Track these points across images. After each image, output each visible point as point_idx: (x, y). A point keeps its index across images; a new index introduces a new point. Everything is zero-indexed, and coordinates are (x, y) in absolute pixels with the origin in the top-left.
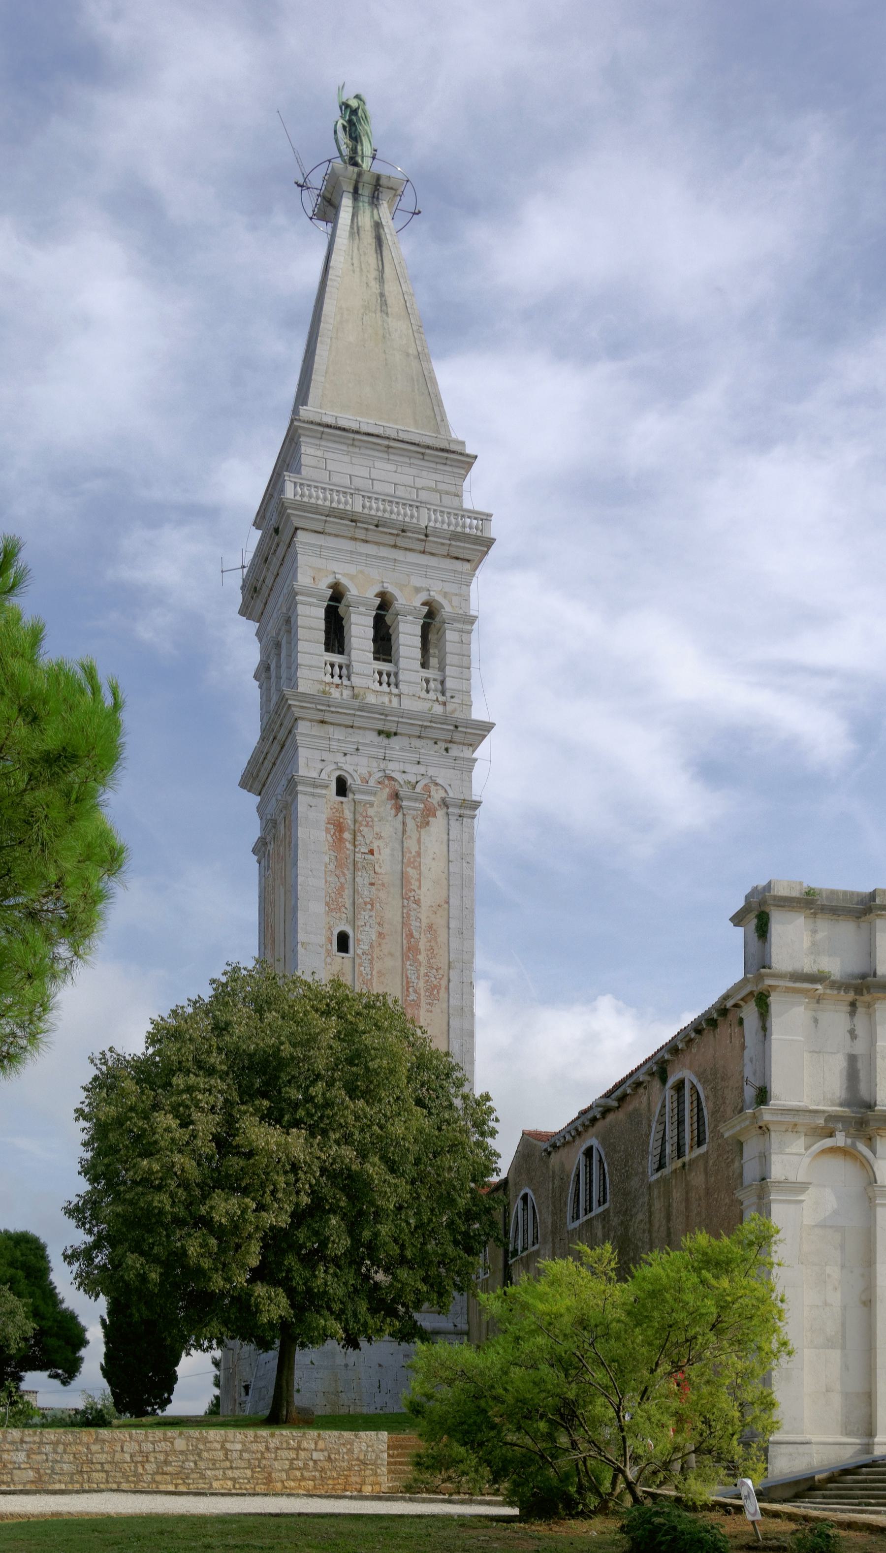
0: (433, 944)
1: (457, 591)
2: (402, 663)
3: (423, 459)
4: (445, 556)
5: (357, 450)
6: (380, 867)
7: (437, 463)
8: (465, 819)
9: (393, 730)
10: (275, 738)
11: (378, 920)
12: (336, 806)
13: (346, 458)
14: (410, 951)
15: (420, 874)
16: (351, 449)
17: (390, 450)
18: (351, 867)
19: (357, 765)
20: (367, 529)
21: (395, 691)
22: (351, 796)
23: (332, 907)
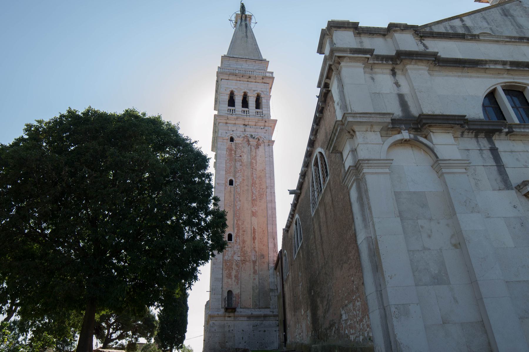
0: (261, 182)
1: (266, 90)
2: (250, 108)
6: (243, 160)
9: (247, 124)
10: (216, 132)
11: (243, 175)
14: (253, 184)
15: (256, 162)
17: (247, 62)
18: (234, 161)
19: (237, 133)
21: (248, 114)
22: (234, 141)
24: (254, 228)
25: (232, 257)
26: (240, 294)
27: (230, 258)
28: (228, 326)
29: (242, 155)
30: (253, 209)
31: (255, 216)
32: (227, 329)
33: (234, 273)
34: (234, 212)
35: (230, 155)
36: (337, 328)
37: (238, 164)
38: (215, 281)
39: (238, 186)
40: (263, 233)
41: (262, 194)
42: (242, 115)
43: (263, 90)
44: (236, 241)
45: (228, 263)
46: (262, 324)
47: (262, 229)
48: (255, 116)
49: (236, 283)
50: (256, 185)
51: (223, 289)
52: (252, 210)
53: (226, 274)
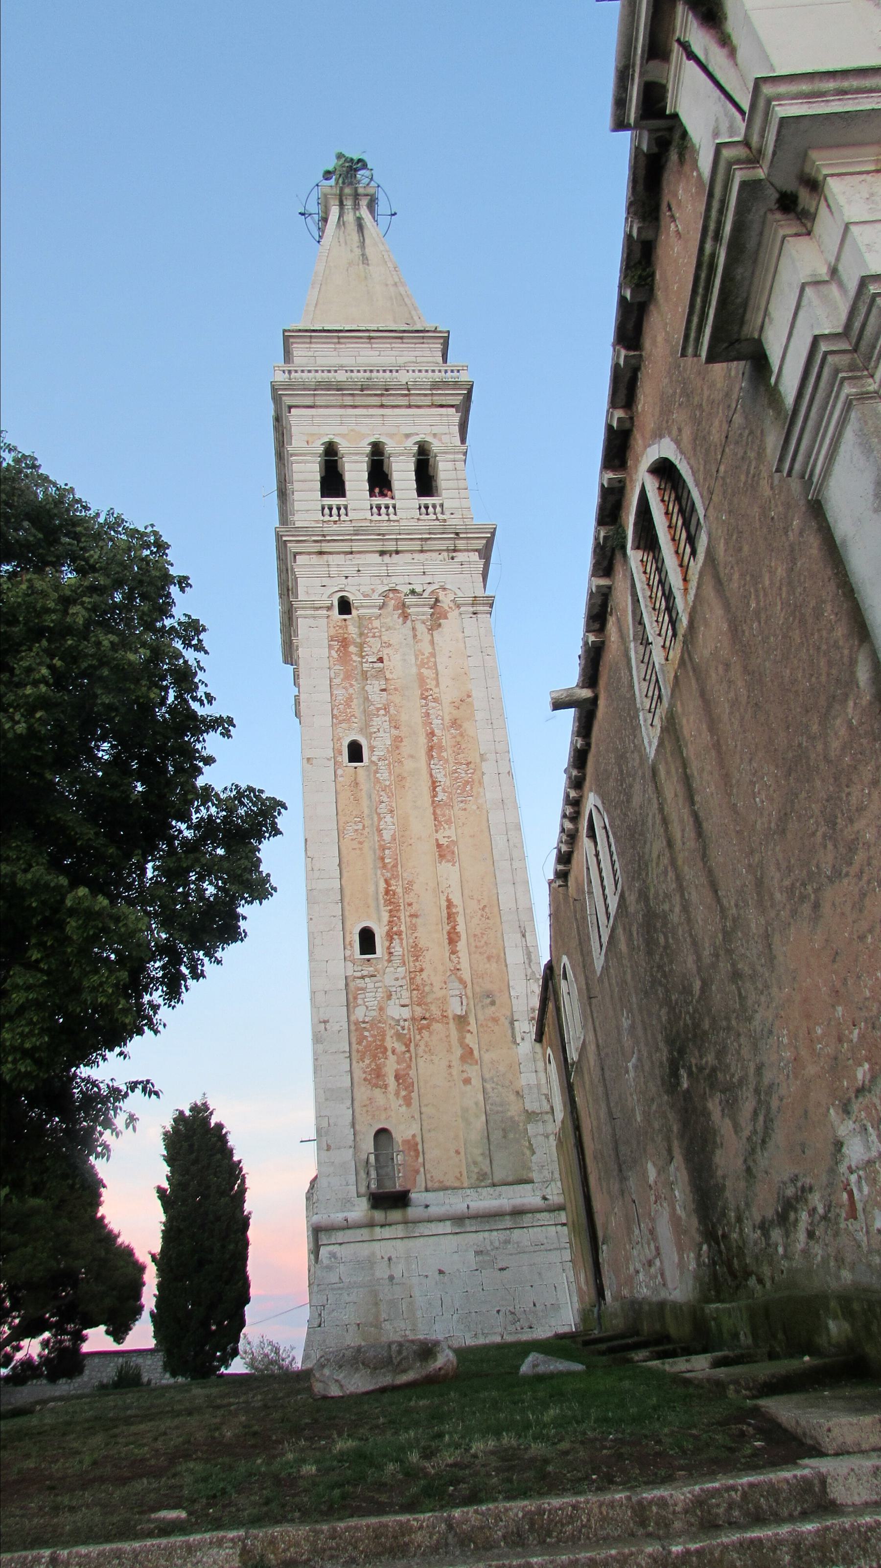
1: (447, 431)
3: (403, 343)
4: (429, 406)
5: (343, 346)
7: (416, 344)
8: (479, 616)
12: (338, 624)
13: (335, 353)
15: (437, 675)
16: (337, 346)
17: (372, 341)
18: (359, 677)
20: (352, 395)
21: (392, 517)
22: (354, 612)
23: (341, 718)
24: (449, 901)
25: (381, 1009)
26: (419, 1139)
27: (374, 1013)
28: (386, 1259)
29: (385, 658)
30: (439, 836)
31: (448, 861)
32: (381, 1272)
33: (391, 1066)
34: (375, 853)
35: (344, 656)
36: (821, 1210)
37: (373, 688)
38: (327, 1100)
39: (380, 764)
40: (482, 916)
41: (467, 782)
42: (371, 521)
43: (435, 430)
44: (391, 953)
45: (366, 1034)
46: (507, 1242)
47: (479, 901)
48: (418, 519)
49: (401, 1102)
50: (444, 754)
51: (357, 1127)
52: (437, 840)
53: (365, 1072)
